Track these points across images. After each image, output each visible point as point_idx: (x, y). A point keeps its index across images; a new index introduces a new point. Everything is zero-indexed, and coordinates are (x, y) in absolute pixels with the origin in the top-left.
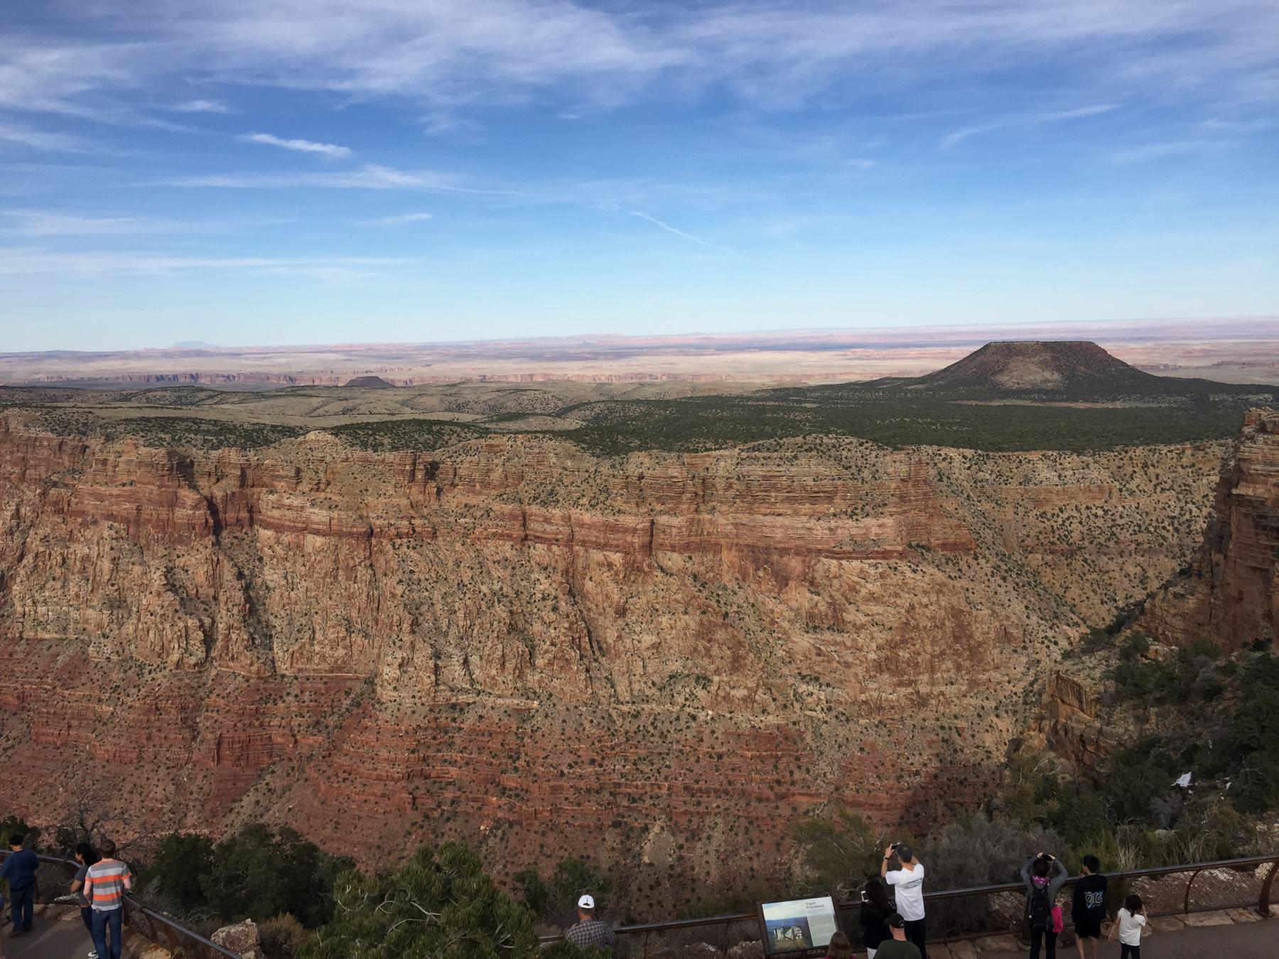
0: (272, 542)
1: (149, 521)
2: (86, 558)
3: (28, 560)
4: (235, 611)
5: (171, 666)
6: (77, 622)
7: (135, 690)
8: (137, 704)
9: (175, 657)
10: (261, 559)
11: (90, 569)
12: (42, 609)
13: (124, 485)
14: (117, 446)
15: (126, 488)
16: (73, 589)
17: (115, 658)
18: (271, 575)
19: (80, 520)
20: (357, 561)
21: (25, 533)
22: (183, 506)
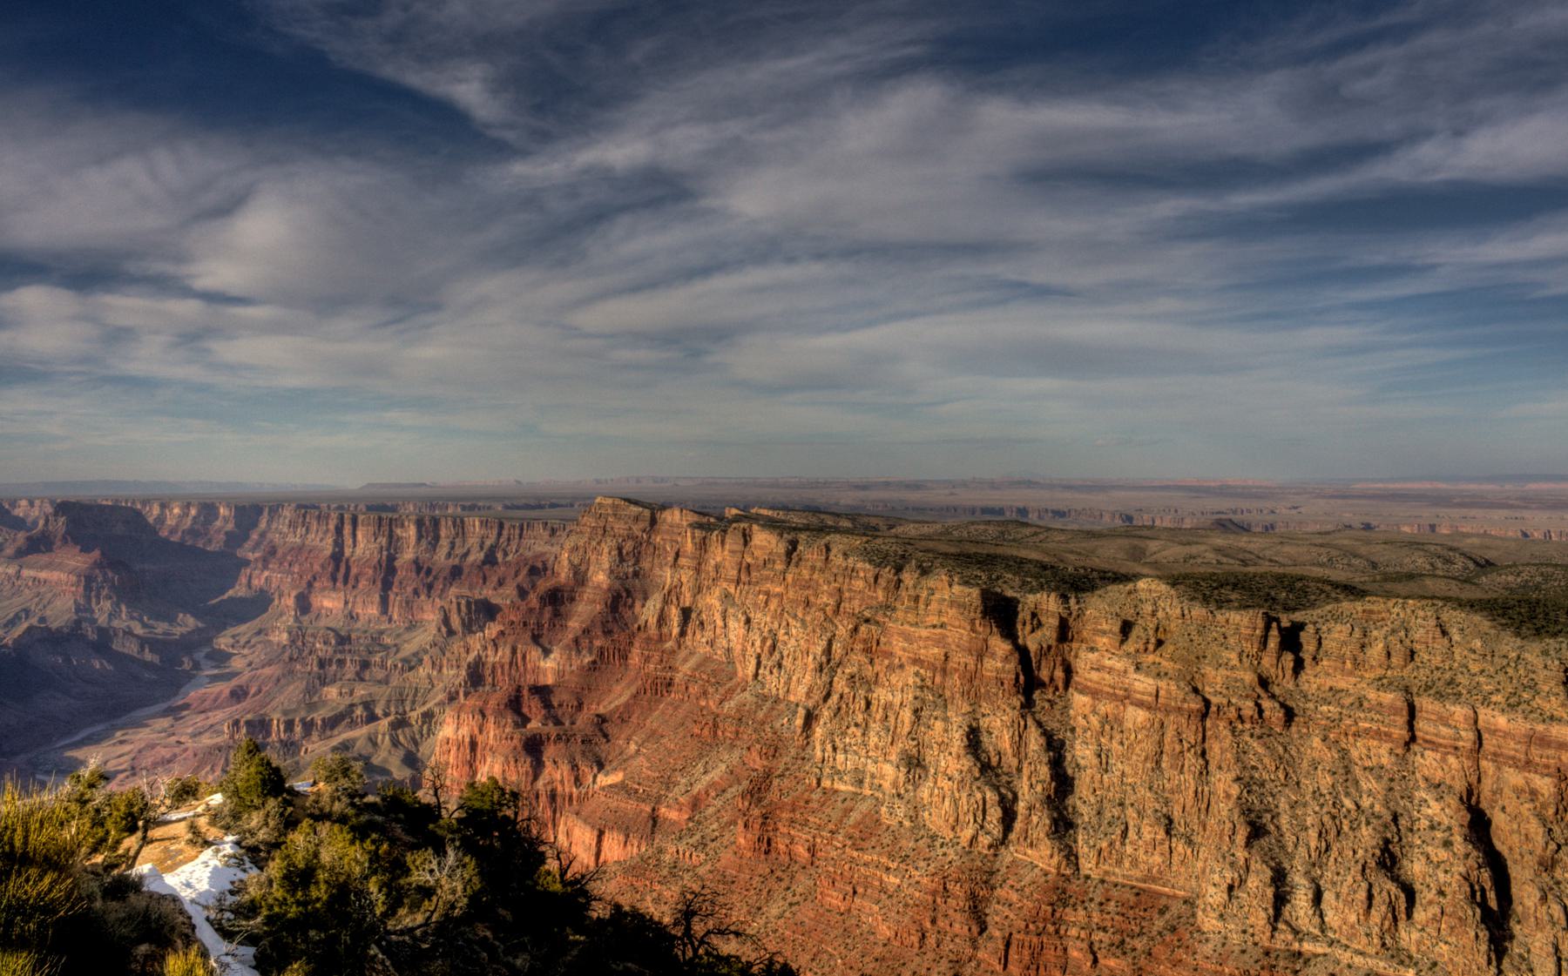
0: (1087, 710)
1: (956, 670)
2: (887, 707)
3: (835, 698)
4: (1039, 788)
5: (964, 842)
6: (873, 776)
7: (922, 864)
8: (925, 880)
9: (968, 833)
10: (1073, 730)
11: (892, 719)
12: (840, 757)
13: (934, 627)
14: (931, 582)
15: (938, 631)
16: (873, 740)
17: (907, 823)
18: (1082, 753)
19: (886, 662)
20: (1186, 745)
21: (833, 671)
22: (993, 655)
